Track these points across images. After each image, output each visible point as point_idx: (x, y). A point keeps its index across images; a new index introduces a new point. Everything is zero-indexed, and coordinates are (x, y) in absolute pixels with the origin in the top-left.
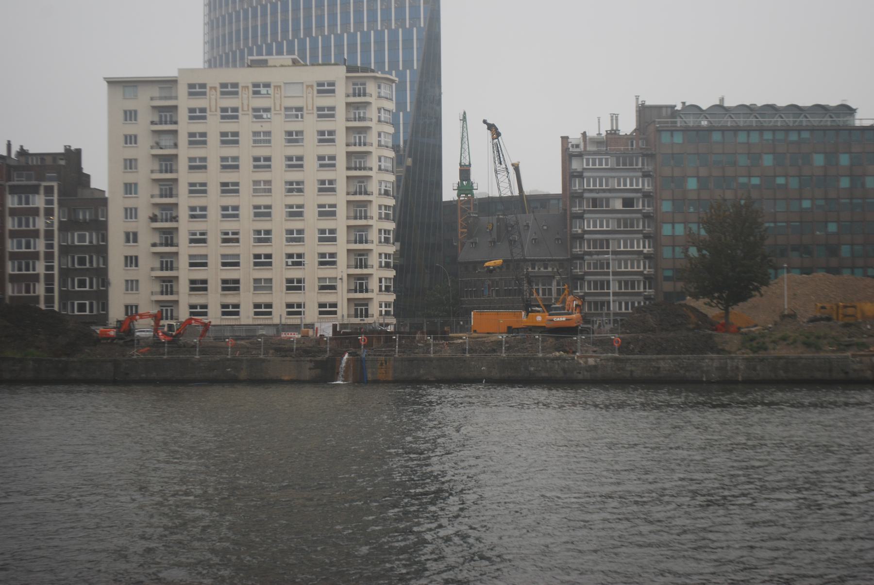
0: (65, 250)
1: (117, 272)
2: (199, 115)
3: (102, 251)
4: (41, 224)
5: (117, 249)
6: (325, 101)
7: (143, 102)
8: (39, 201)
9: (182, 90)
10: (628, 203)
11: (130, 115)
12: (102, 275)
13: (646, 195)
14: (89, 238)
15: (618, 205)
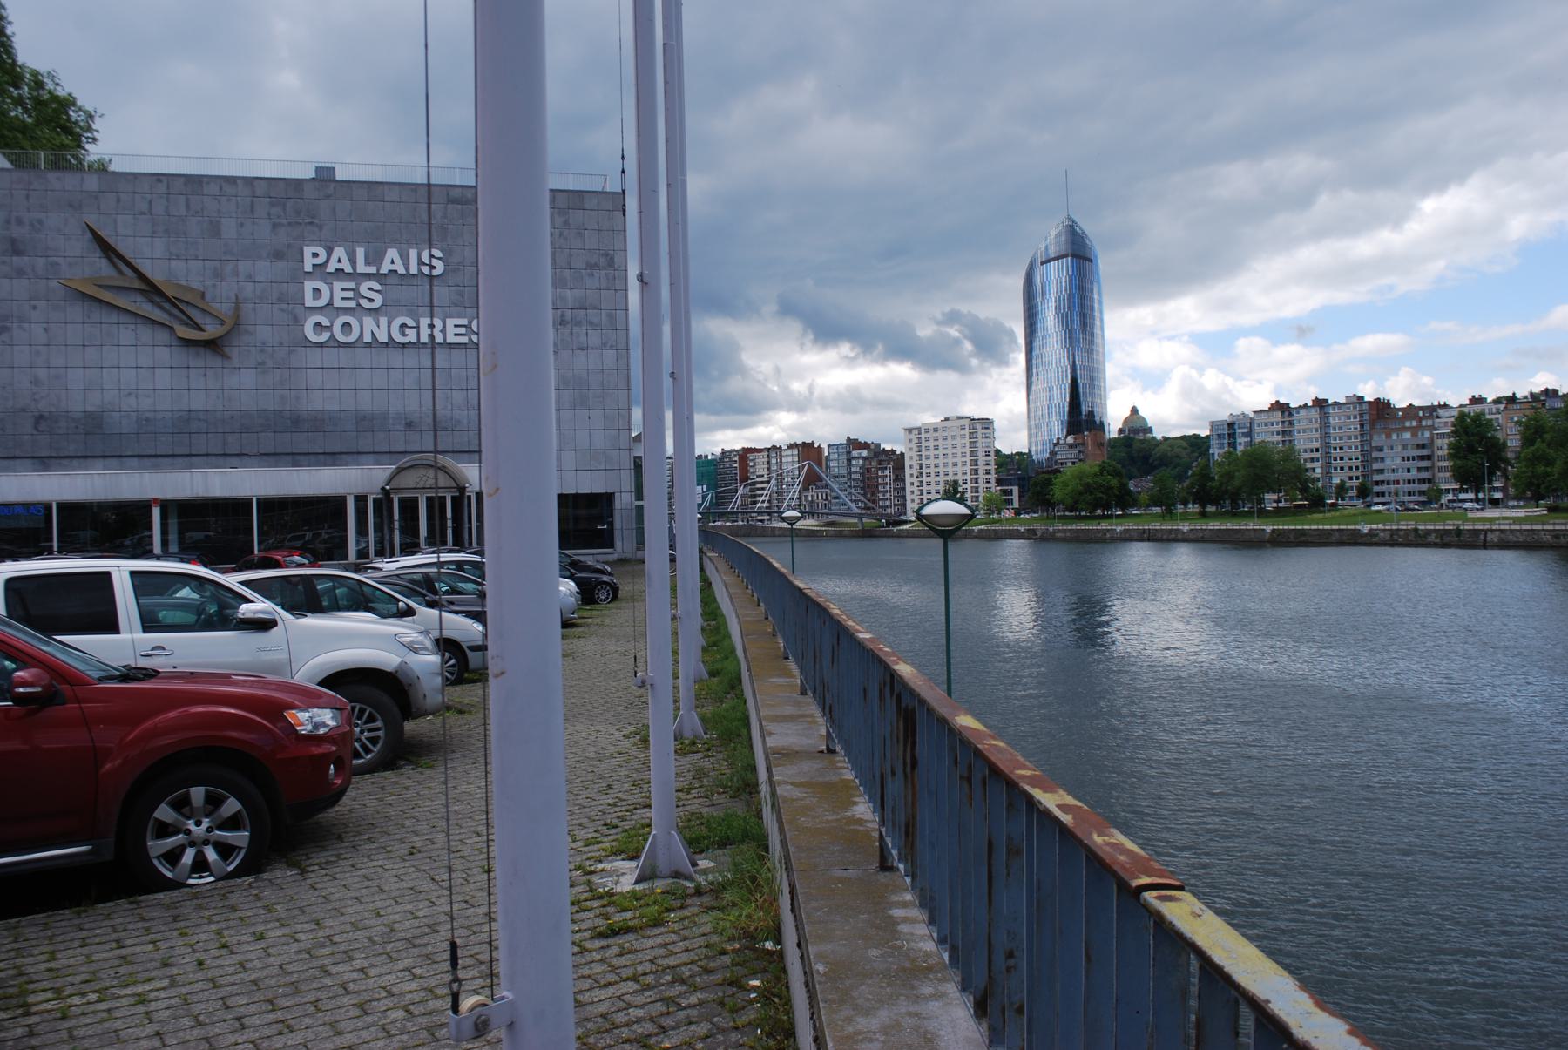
0: (894, 489)
1: (909, 497)
2: (927, 440)
3: (904, 489)
4: (888, 480)
5: (908, 488)
6: (962, 432)
7: (913, 436)
8: (887, 472)
9: (923, 431)
10: (1073, 463)
11: (910, 441)
12: (904, 497)
13: (1080, 460)
14: (901, 485)
15: (1070, 464)
